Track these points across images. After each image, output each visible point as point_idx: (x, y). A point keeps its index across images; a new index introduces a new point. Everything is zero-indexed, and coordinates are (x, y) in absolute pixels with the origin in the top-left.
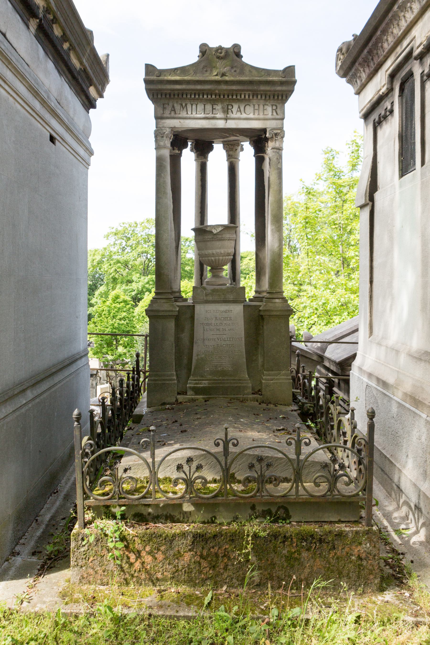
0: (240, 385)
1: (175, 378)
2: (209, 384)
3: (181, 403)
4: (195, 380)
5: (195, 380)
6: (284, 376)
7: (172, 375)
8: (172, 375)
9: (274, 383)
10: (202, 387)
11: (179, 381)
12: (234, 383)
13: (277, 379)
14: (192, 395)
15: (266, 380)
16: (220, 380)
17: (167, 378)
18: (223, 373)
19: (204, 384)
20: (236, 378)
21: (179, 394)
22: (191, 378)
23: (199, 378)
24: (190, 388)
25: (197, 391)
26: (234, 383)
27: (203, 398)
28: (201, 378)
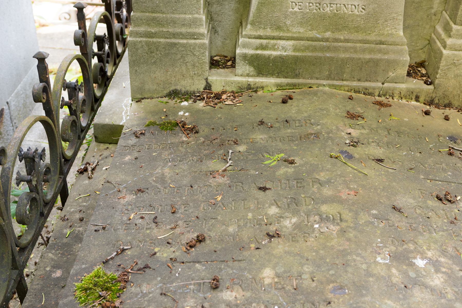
0: (378, 56)
1: (204, 30)
2: (296, 49)
3: (218, 96)
4: (260, 37)
5: (260, 37)
7: (195, 22)
8: (195, 22)
10: (276, 57)
11: (213, 30)
12: (364, 51)
14: (248, 75)
15: (454, 48)
16: (327, 40)
17: (183, 30)
18: (338, 22)
19: (284, 49)
20: (372, 37)
21: (214, 64)
22: (248, 30)
23: (269, 32)
24: (245, 57)
25: (262, 66)
26: (364, 51)
27: (280, 87)
28: (276, 34)
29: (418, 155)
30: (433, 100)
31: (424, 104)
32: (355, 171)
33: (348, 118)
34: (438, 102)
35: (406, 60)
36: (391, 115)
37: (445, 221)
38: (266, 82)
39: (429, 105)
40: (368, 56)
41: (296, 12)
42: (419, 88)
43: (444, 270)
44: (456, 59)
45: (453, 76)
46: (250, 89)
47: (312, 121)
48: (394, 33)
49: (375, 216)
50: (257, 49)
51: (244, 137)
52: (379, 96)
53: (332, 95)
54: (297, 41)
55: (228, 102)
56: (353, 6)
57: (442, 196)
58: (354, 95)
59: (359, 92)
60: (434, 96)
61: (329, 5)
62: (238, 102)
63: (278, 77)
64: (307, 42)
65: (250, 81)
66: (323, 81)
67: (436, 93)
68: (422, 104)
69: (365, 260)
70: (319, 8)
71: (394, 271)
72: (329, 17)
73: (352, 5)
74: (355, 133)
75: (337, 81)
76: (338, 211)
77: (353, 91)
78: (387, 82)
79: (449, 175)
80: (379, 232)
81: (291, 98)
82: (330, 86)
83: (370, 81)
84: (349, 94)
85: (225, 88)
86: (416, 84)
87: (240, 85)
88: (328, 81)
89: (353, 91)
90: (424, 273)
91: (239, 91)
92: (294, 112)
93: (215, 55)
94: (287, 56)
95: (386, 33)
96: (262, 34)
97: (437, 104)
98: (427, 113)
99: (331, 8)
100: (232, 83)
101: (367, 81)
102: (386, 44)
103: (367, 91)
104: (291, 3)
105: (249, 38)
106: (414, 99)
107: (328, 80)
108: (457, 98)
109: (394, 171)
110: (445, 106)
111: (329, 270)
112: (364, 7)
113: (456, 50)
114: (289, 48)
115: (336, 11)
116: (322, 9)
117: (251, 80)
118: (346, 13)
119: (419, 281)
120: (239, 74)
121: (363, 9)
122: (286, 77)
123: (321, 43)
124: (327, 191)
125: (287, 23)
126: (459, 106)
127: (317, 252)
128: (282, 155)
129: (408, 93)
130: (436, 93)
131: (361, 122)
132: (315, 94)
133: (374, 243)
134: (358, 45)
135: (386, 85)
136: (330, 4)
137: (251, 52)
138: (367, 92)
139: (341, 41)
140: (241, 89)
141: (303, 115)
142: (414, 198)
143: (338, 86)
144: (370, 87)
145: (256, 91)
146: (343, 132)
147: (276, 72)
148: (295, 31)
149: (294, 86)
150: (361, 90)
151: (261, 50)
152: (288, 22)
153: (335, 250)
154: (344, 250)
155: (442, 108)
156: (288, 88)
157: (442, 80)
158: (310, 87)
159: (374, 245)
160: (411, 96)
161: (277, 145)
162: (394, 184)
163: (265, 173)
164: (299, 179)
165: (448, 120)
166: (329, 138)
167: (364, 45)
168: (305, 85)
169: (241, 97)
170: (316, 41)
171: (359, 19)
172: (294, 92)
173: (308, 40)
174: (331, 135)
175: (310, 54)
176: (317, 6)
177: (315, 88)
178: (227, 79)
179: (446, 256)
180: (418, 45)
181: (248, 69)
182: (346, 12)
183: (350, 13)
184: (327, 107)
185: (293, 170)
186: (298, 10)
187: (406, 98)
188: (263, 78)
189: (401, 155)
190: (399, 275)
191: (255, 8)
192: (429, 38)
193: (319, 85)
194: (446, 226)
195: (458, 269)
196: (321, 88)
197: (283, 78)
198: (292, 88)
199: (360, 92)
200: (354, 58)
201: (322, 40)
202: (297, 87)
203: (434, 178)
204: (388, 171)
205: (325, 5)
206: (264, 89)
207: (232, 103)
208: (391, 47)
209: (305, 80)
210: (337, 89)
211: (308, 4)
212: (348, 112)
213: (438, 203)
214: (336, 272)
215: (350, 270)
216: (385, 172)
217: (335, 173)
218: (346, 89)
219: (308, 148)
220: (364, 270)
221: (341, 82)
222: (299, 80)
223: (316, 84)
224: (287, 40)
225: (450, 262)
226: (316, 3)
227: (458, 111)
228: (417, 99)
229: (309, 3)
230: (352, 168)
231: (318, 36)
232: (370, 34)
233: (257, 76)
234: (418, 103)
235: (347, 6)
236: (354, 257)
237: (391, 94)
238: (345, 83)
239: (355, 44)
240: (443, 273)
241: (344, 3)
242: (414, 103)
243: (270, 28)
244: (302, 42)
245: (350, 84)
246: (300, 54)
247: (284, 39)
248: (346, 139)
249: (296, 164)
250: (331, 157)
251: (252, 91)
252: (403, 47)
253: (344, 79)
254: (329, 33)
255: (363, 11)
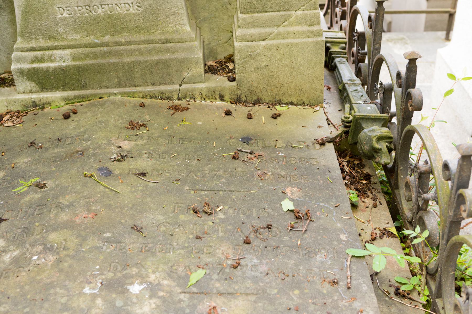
0: (166, 56)
2: (75, 58)
4: (33, 49)
5: (33, 49)
6: (299, 23)
9: (269, 48)
10: (55, 69)
12: (150, 52)
13: (280, 36)
14: (31, 92)
15: (243, 39)
16: (107, 45)
18: (114, 23)
19: (62, 59)
22: (20, 43)
23: (42, 43)
24: (21, 72)
26: (150, 52)
27: (68, 100)
28: (50, 43)
29: (195, 162)
30: (240, 97)
31: (231, 102)
32: (107, 190)
33: (128, 128)
34: (245, 99)
35: (198, 57)
36: (183, 120)
37: (191, 236)
38: (52, 97)
39: (236, 103)
40: (155, 58)
41: (66, 18)
42: (220, 87)
43: (161, 294)
44: (250, 51)
45: (253, 69)
46: (36, 106)
47: (86, 136)
48: (180, 29)
49: (108, 241)
50: (33, 62)
51: (7, 162)
52: (179, 99)
53: (122, 104)
54: (75, 50)
55: (10, 124)
56: (127, 5)
57: (200, 208)
58: (147, 101)
59: (156, 98)
60: (239, 94)
61: (100, 7)
62: (18, 123)
63: (64, 90)
64: (86, 49)
65: (34, 98)
66: (115, 89)
67: (240, 90)
68: (229, 103)
69: (69, 292)
70: (90, 11)
71: (99, 301)
72: (103, 19)
73: (125, 4)
74: (126, 145)
75: (130, 88)
76: (65, 238)
77: (148, 97)
78: (185, 83)
79: (222, 183)
80: (102, 258)
81: (75, 113)
82: (123, 94)
83: (165, 84)
84: (143, 100)
85: (9, 108)
86: (220, 82)
87: (24, 103)
88: (120, 89)
89: (148, 97)
90: (135, 300)
91: (25, 109)
92: (71, 128)
93: (3, 72)
94: (67, 66)
95: (170, 30)
96: (34, 46)
97: (245, 101)
98: (228, 113)
99: (103, 10)
100: (15, 102)
101: (162, 84)
102: (173, 42)
103: (164, 95)
104: (57, 9)
105: (22, 51)
106: (218, 99)
107: (119, 87)
108: (264, 92)
109: (155, 184)
110: (255, 103)
111: (25, 307)
112: (139, 5)
113: (248, 41)
114: (67, 57)
115: (109, 13)
116: (93, 12)
117: (34, 96)
118: (120, 13)
119: (124, 310)
120: (21, 92)
121: (138, 6)
122: (73, 90)
123: (102, 48)
124: (64, 217)
125: (59, 30)
126: (271, 101)
127: (22, 288)
128: (37, 179)
129: (210, 93)
130: (240, 90)
131: (143, 131)
132: (102, 105)
133: (89, 271)
134: (142, 46)
135: (183, 86)
136: (101, 5)
137: (26, 66)
138: (164, 97)
139: (123, 44)
140: (27, 107)
141: (79, 131)
142: (165, 214)
143: (130, 93)
144: (166, 91)
145: (43, 108)
146: (114, 145)
147: (60, 85)
148: (70, 38)
149: (83, 98)
150: (157, 95)
151: (38, 63)
152: (61, 30)
153: (42, 284)
154: (52, 282)
155: (251, 105)
156: (77, 101)
157: (242, 74)
158: (101, 98)
159: (89, 273)
160: (214, 96)
161: (36, 169)
162: (149, 199)
163: (10, 202)
164: (41, 205)
165: (250, 118)
166: (95, 155)
167: (149, 45)
168: (95, 96)
169: (25, 117)
170: (95, 47)
171: (137, 18)
172: (82, 105)
173: (87, 47)
174: (97, 151)
175: (91, 62)
176: (87, 9)
177: (106, 98)
178: (9, 98)
179: (171, 278)
180: (221, 38)
181: (29, 85)
182: (121, 12)
183: (126, 12)
184: (109, 118)
185: (40, 195)
186: (68, 15)
187: (209, 99)
188: (49, 93)
189: (172, 165)
190: (103, 305)
191: (20, 18)
192: (231, 29)
193: (109, 95)
194: (189, 243)
195: (180, 291)
196: (112, 97)
197: (70, 90)
198: (81, 100)
199: (156, 97)
200: (140, 61)
201: (101, 45)
202: (87, 99)
203: (201, 188)
204: (147, 186)
205: (95, 7)
206: (52, 104)
207: (12, 125)
208: (179, 45)
209: (94, 90)
210: (131, 97)
211: (76, 8)
212: (131, 121)
213: (194, 218)
214: (31, 309)
215: (46, 305)
216: (143, 186)
217: (81, 195)
218: (141, 95)
219: (67, 168)
220: (62, 304)
221: (134, 88)
222: (88, 91)
223: (106, 93)
224: (64, 49)
225: (174, 284)
226: (85, 6)
227: (269, 107)
228: (222, 98)
229: (78, 7)
230: (104, 186)
231: (96, 41)
232: (153, 33)
233: (41, 91)
234: (224, 103)
235: (119, 5)
236: (58, 290)
237: (192, 96)
238: (138, 89)
239: (139, 46)
240: (159, 297)
241: (116, 3)
242: (219, 103)
243: (43, 38)
244: (80, 50)
245: (144, 90)
246: (81, 63)
247: (60, 49)
248: (113, 154)
249: (46, 189)
250: (85, 176)
251: (39, 109)
252: (192, 43)
253: (136, 85)
254: (108, 36)
255: (140, 9)
